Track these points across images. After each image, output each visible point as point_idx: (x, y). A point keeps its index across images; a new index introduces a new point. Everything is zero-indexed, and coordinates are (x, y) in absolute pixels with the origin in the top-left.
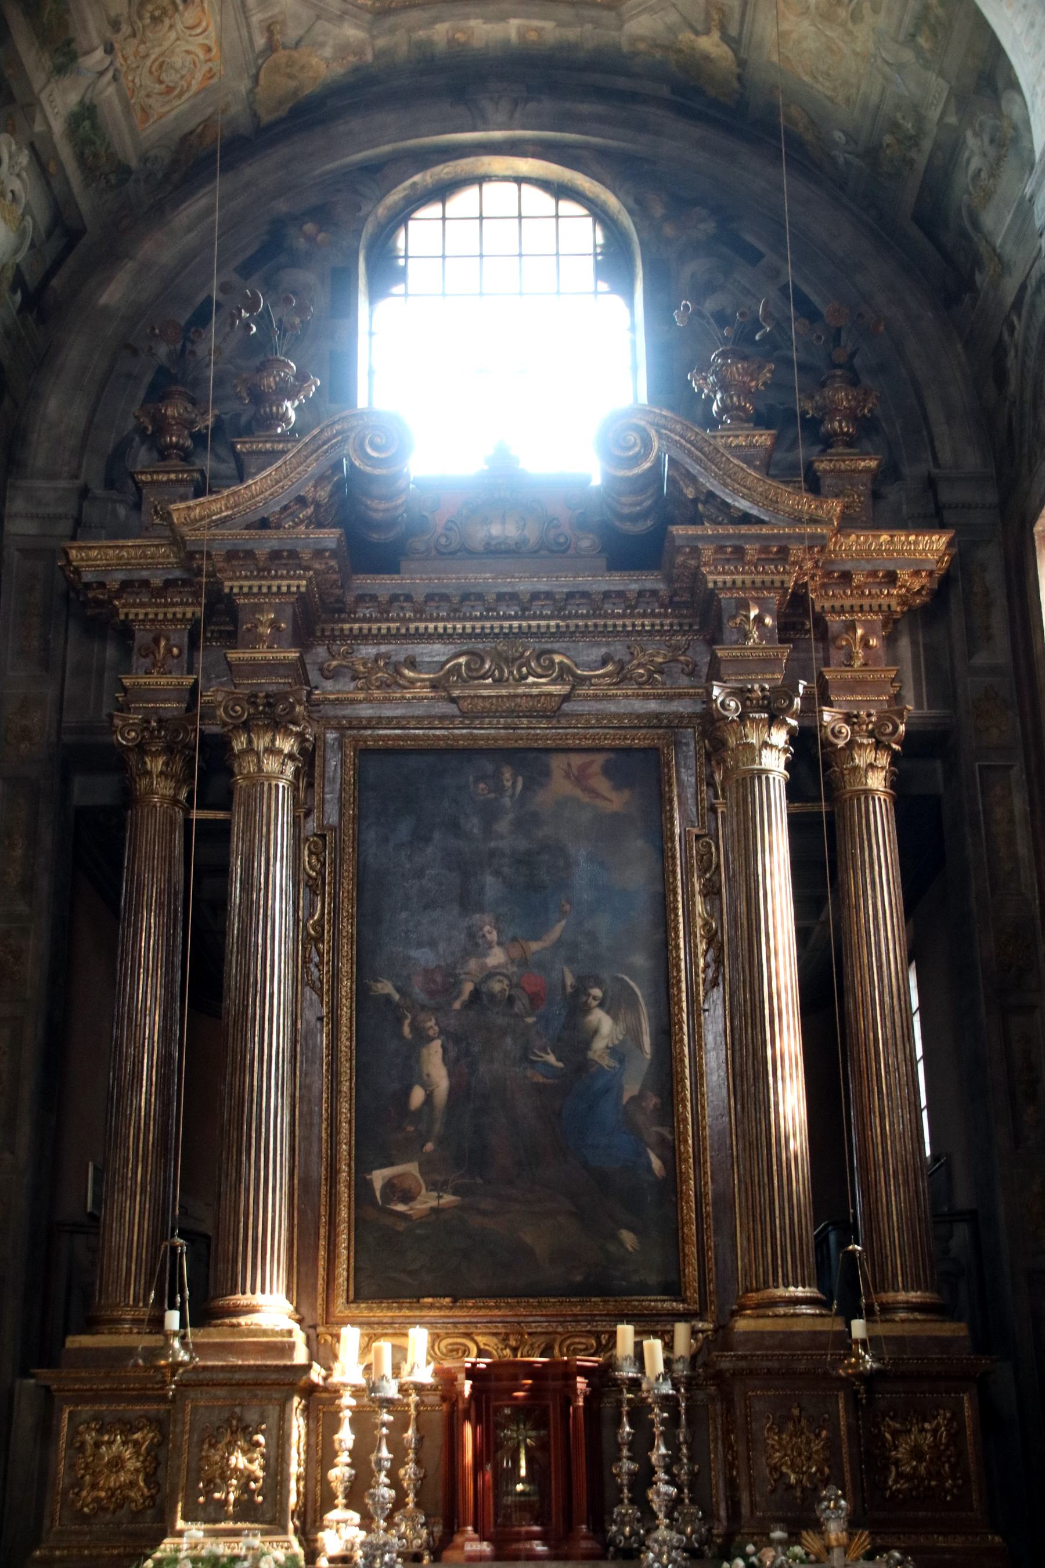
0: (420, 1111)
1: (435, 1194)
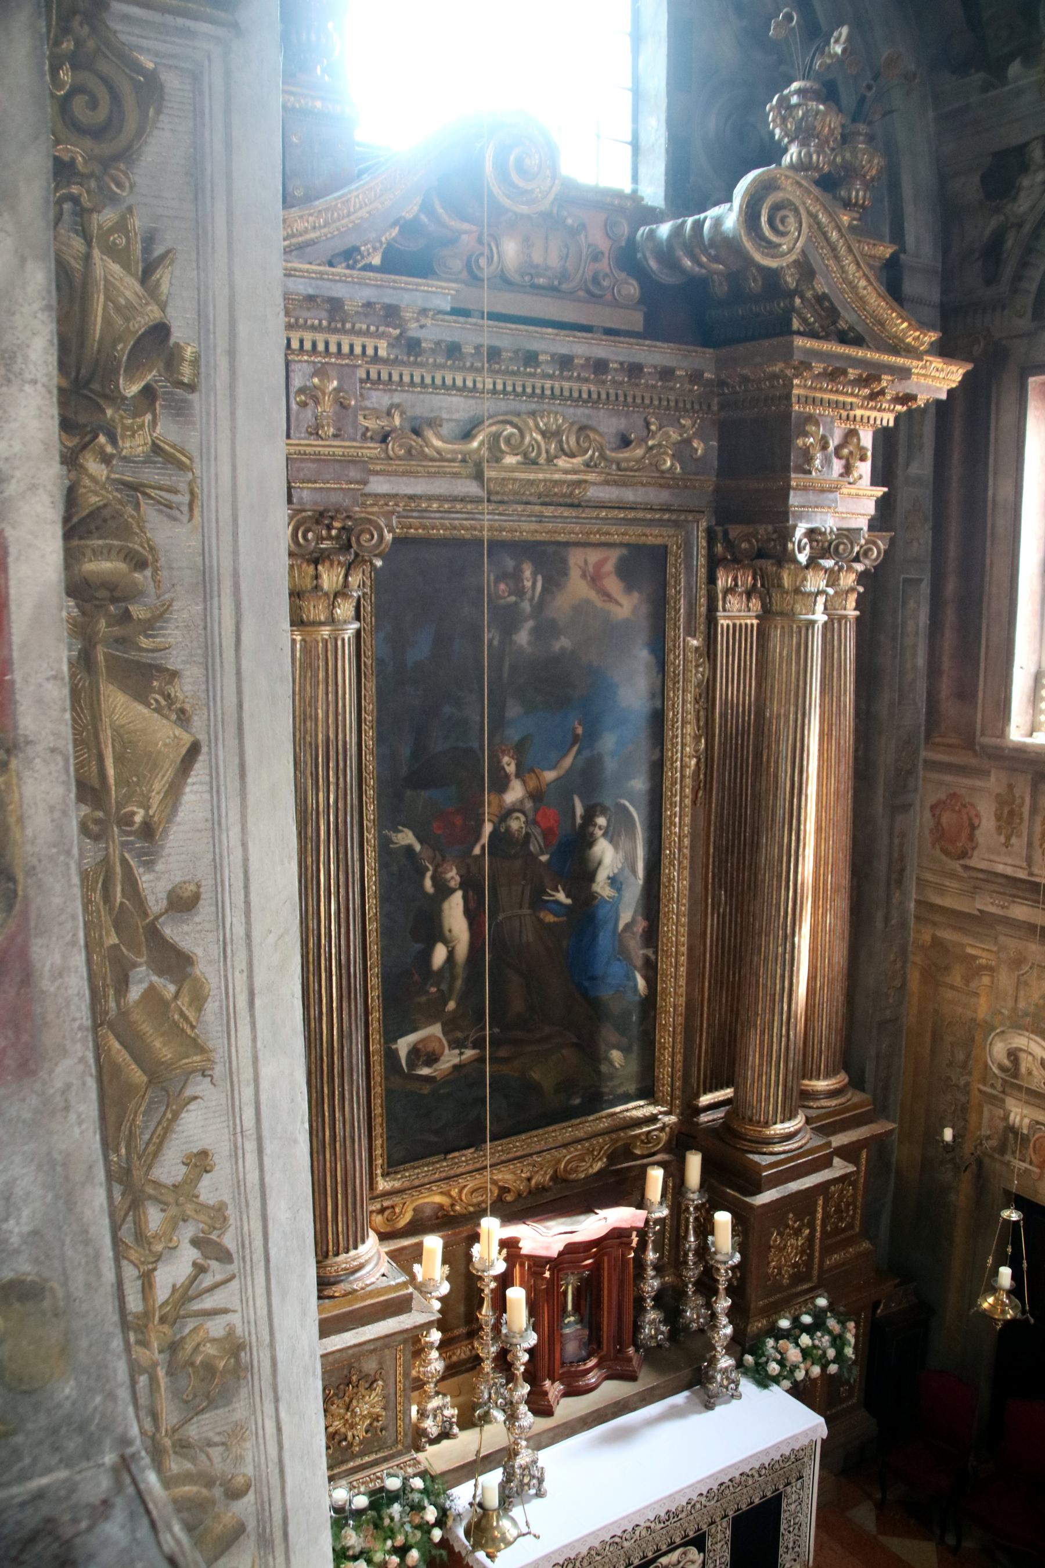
0: (441, 969)
1: (457, 1051)
